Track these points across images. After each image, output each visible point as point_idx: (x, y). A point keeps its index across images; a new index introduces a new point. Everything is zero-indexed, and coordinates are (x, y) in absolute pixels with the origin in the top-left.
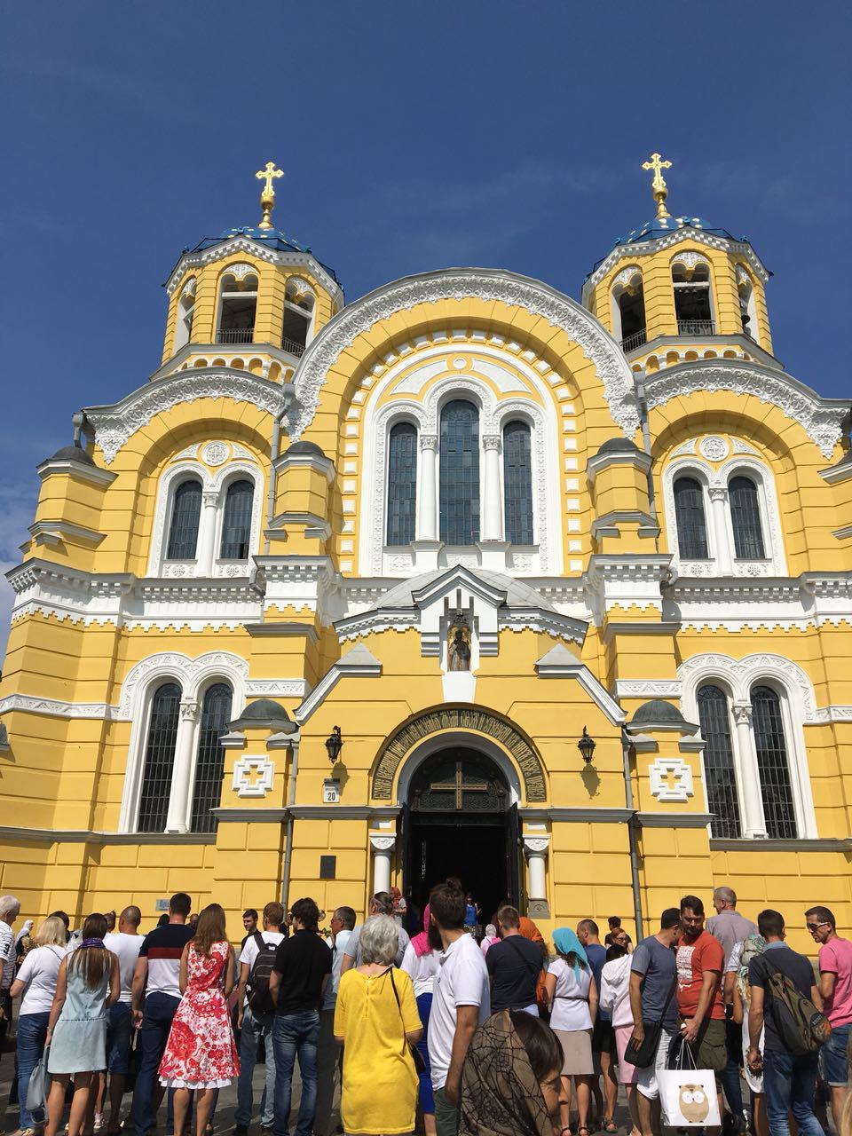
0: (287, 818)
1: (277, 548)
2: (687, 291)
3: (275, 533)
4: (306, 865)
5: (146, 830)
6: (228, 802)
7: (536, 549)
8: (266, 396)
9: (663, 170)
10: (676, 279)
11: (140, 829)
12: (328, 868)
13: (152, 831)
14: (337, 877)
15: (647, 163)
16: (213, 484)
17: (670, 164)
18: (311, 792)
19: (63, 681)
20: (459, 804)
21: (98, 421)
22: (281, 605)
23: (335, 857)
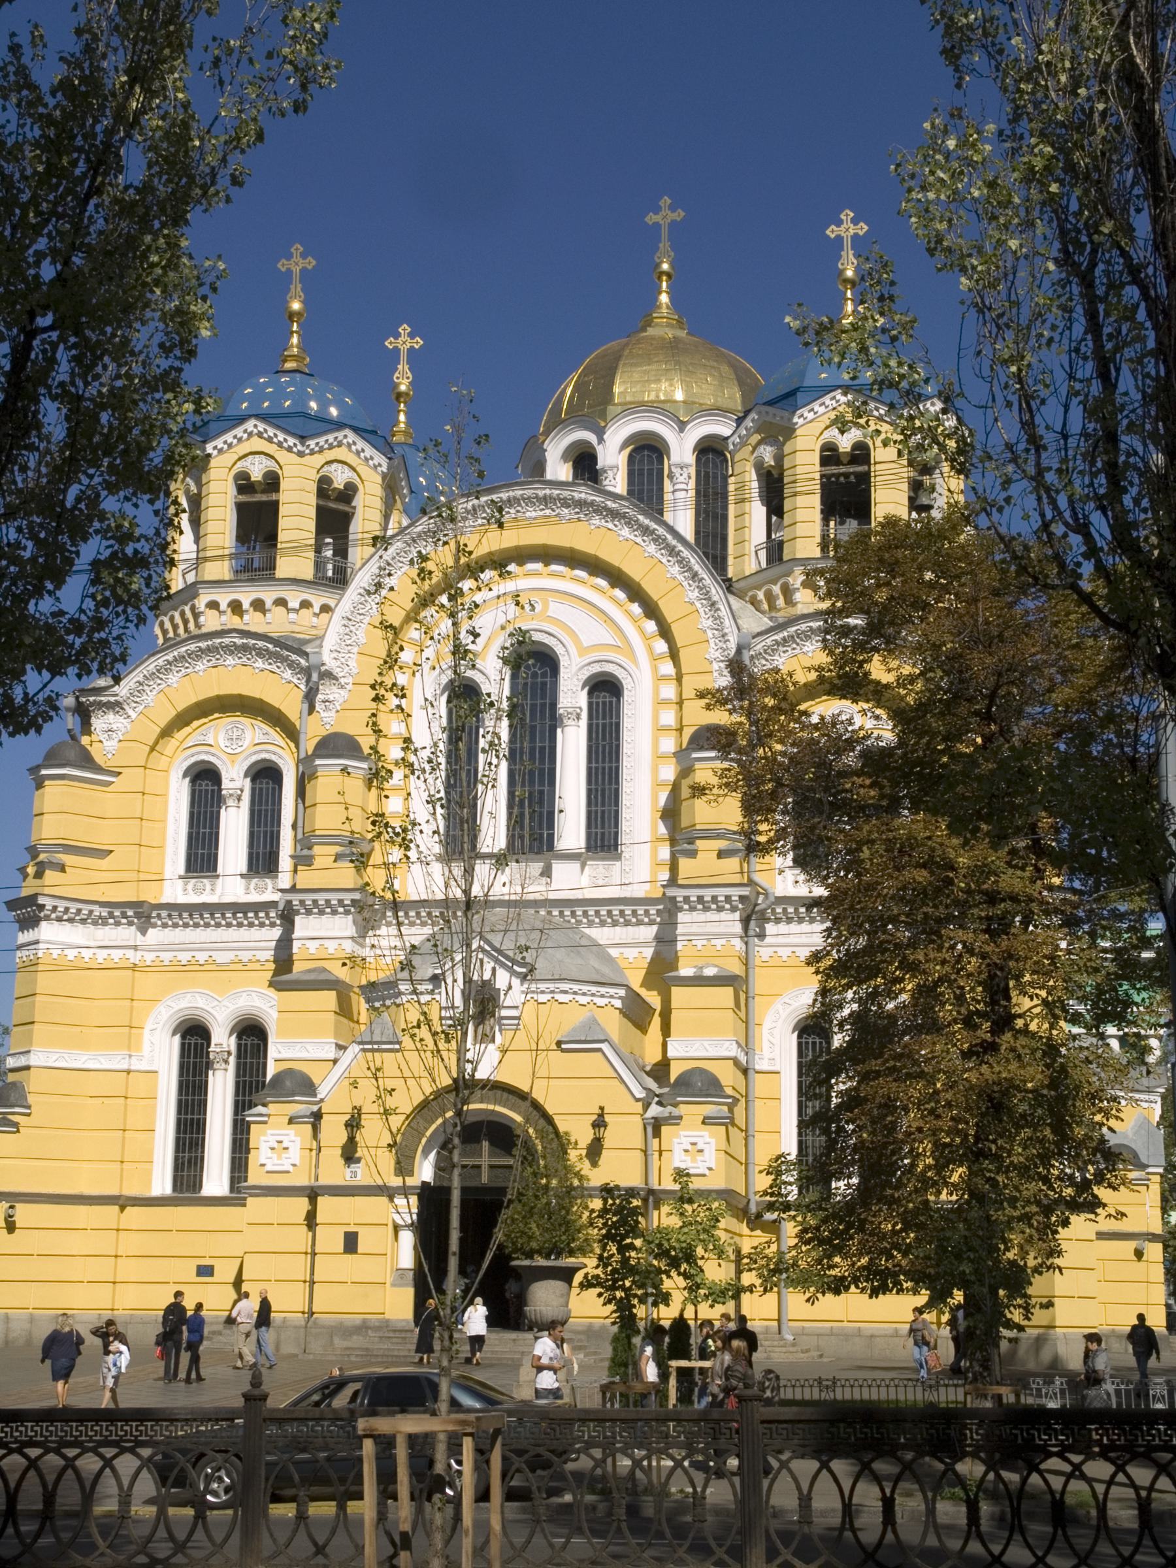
0: (313, 1194)
1: (306, 878)
2: (842, 479)
3: (302, 860)
4: (330, 1239)
5: (181, 1191)
6: (255, 1177)
7: (618, 857)
8: (292, 665)
9: (855, 237)
10: (824, 461)
11: (175, 1189)
12: (351, 1243)
13: (188, 1191)
14: (361, 1248)
15: (833, 227)
16: (234, 779)
17: (866, 228)
18: (334, 1172)
19: (79, 1029)
20: (484, 1179)
21: (92, 704)
22: (313, 946)
23: (355, 1235)
